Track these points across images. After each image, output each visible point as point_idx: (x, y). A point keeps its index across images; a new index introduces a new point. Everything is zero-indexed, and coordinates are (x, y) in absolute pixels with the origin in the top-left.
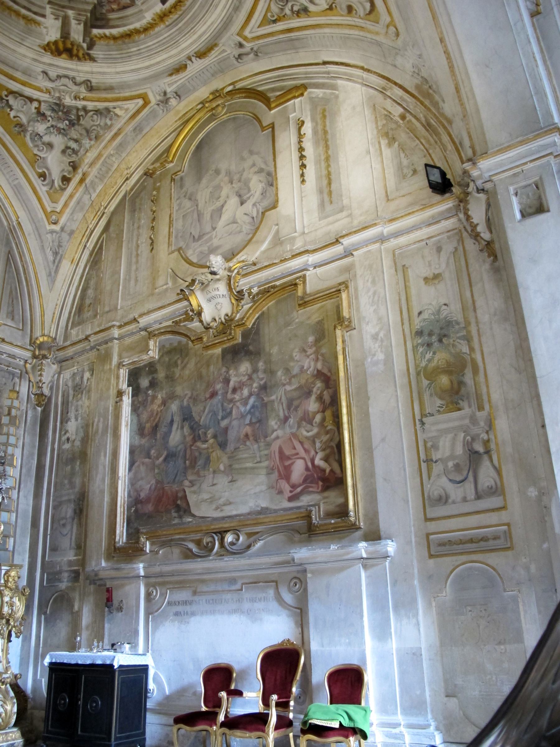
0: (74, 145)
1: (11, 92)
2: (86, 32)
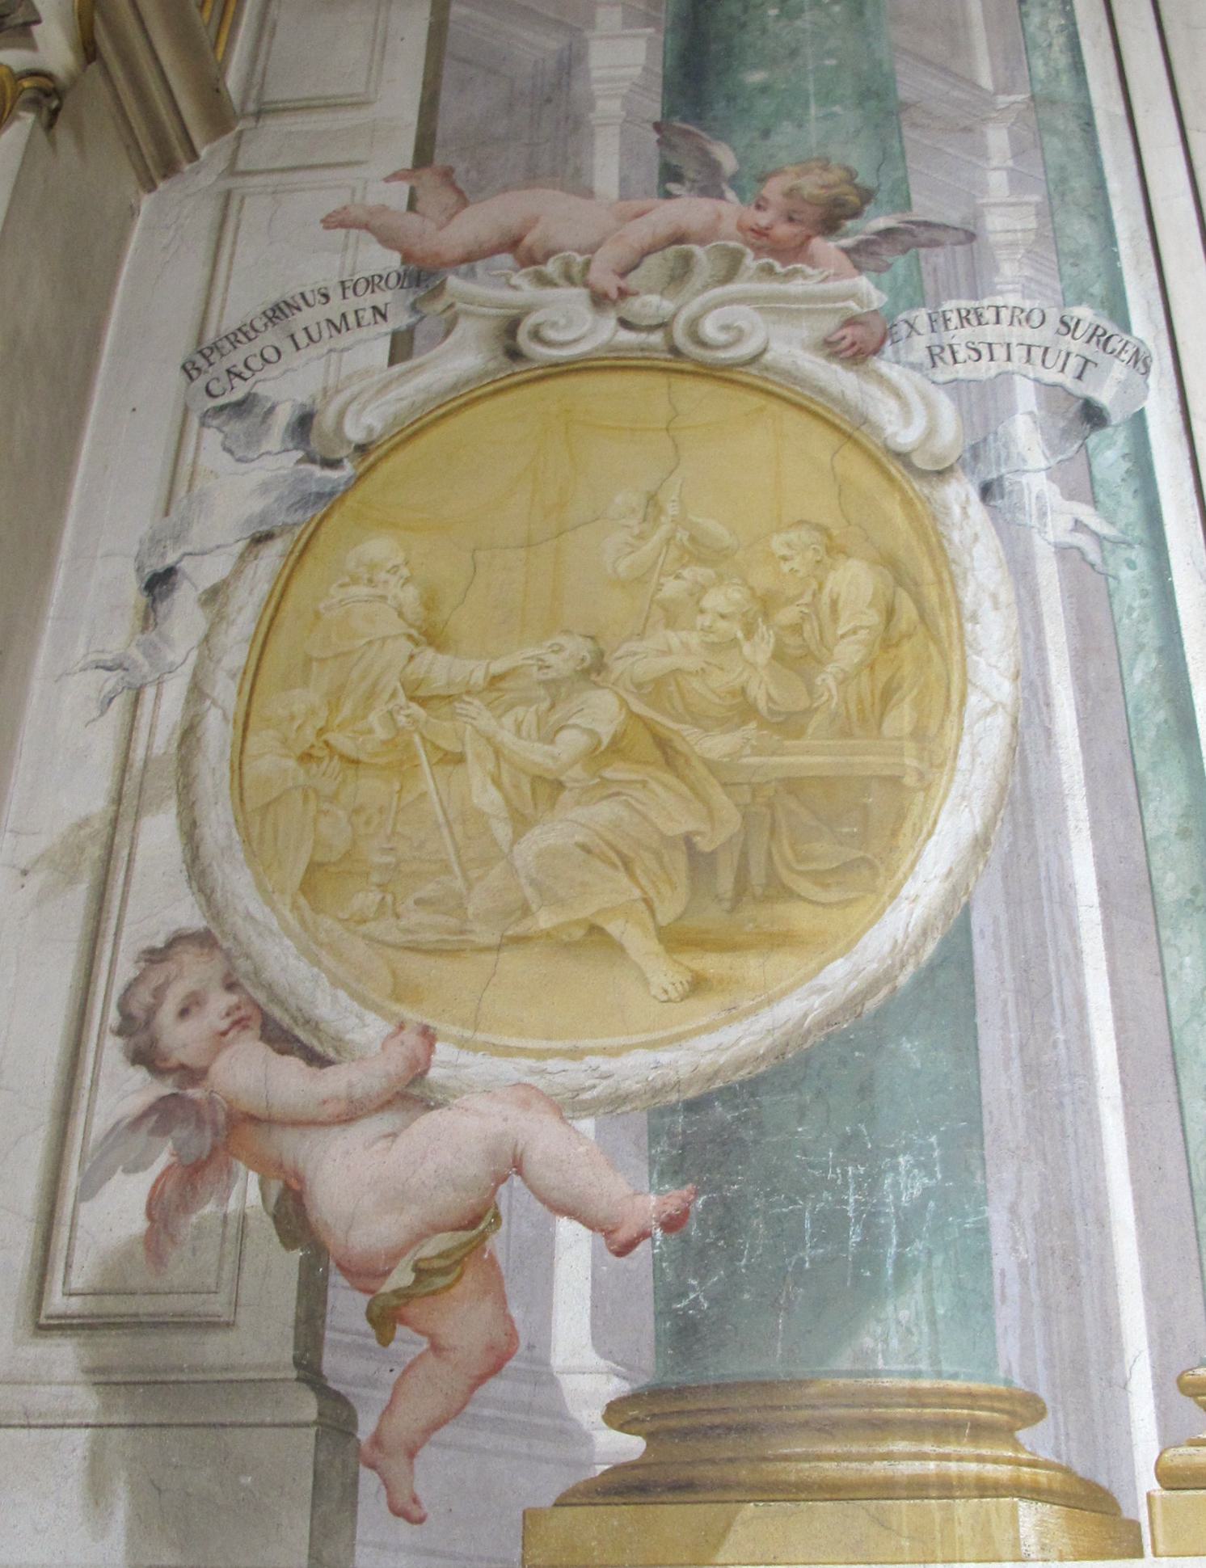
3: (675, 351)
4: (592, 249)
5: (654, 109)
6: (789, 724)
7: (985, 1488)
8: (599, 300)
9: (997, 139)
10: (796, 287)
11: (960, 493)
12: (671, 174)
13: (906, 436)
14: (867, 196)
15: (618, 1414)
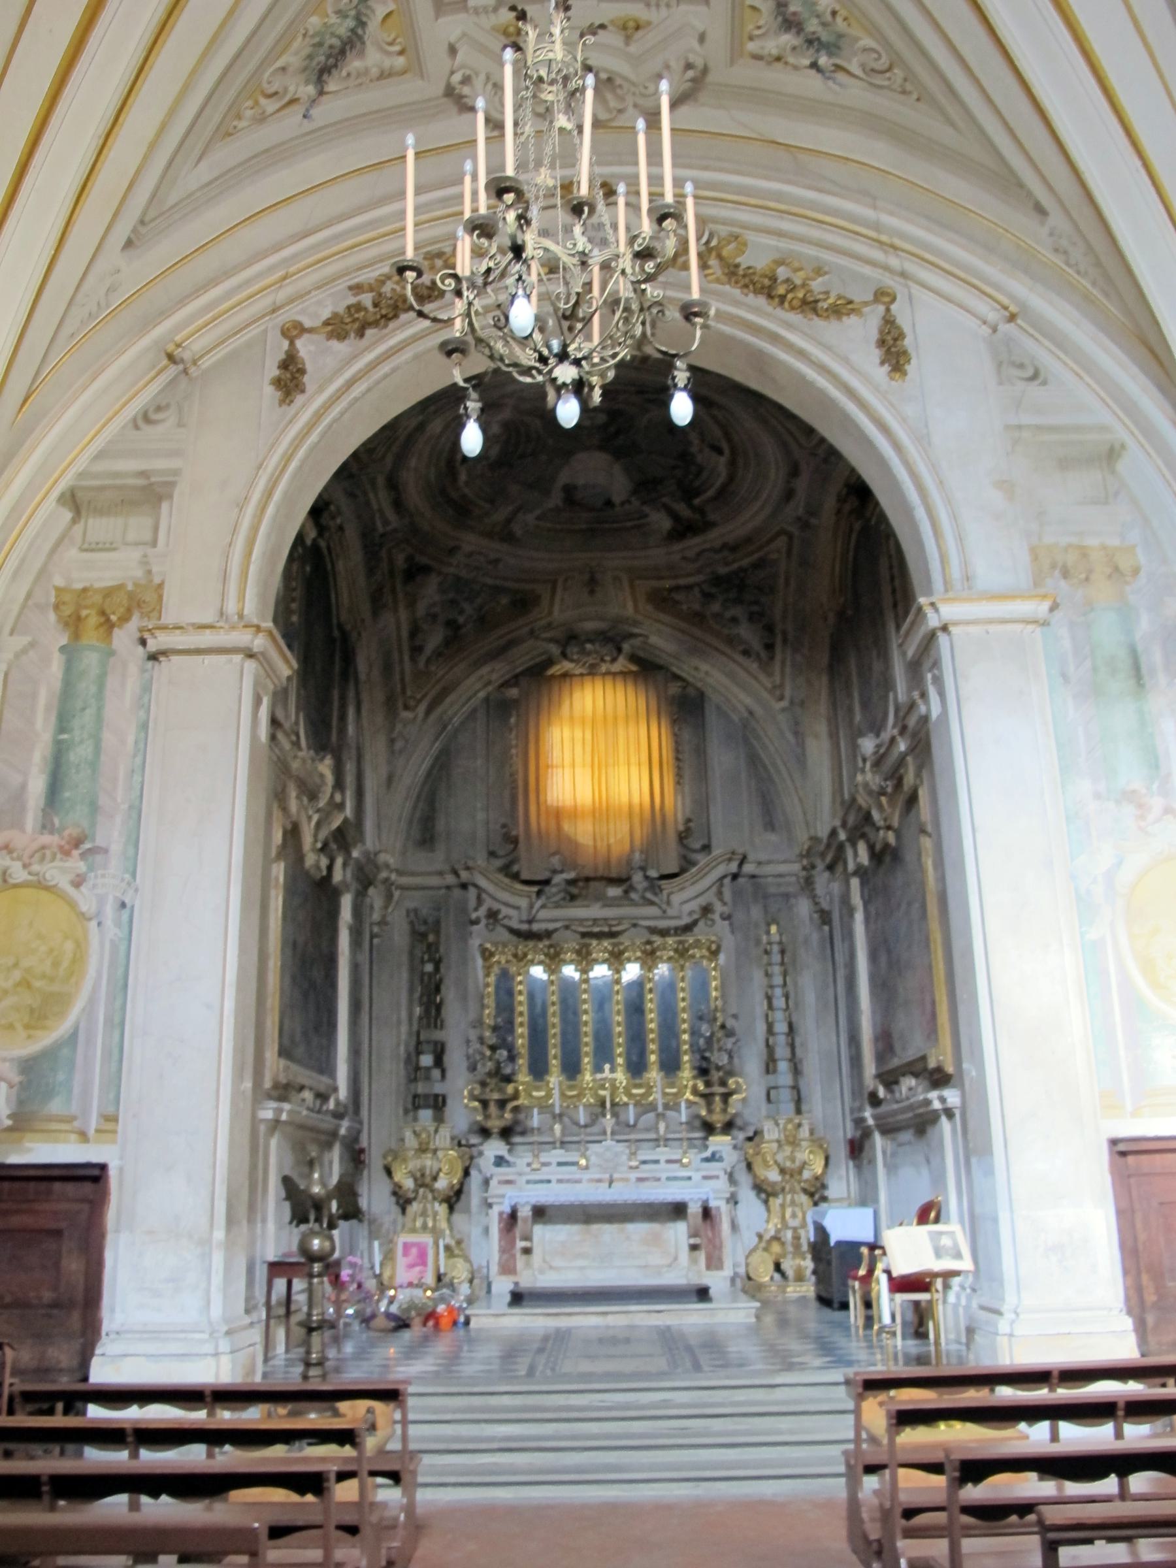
0: (755, 608)
1: (671, 590)
2: (691, 506)
3: (39, 882)
4: (24, 850)
5: (42, 803)
6: (52, 979)
7: (66, 1131)
8: (25, 866)
9: (118, 819)
10: (67, 864)
11: (93, 924)
12: (44, 827)
13: (84, 908)
14: (86, 837)
15: (9, 1117)
